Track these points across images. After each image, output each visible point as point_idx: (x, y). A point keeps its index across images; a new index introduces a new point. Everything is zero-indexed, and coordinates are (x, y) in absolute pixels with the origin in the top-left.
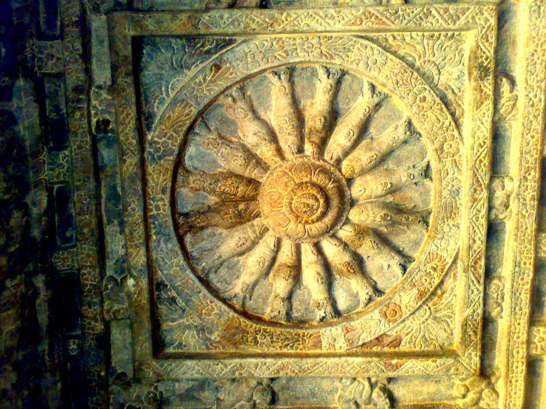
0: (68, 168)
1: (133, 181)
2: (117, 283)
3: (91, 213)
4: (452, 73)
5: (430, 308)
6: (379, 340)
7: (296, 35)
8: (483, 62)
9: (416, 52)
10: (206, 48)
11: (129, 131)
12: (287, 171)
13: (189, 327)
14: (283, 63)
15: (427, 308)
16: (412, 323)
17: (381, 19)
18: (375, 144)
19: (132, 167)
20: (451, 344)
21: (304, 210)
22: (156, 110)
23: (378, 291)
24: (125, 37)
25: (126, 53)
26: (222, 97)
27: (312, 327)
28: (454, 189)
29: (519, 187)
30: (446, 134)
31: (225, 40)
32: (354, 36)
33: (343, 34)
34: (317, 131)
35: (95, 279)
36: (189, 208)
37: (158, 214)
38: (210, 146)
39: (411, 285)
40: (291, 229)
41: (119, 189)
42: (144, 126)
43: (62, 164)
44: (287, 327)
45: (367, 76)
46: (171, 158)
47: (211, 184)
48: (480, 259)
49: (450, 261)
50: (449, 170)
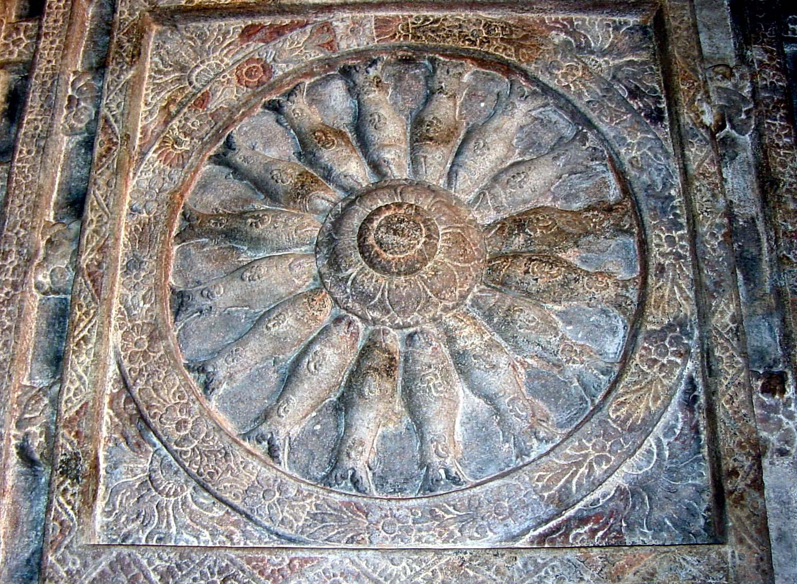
2: (730, 121)
3: (784, 233)
5: (190, 83)
6: (279, 31)
8: (73, 485)
9: (192, 512)
10: (586, 528)
12: (434, 299)
13: (603, 53)
14: (441, 498)
15: (195, 83)
16: (222, 61)
17: (254, 567)
18: (269, 347)
20: (160, 33)
21: (402, 225)
22: (680, 415)
23: (275, 108)
24: (741, 541)
25: (738, 512)
27: (392, 50)
28: (135, 272)
29: (26, 273)
30: (143, 364)
34: (376, 370)
35: (769, 127)
39: (218, 115)
41: (740, 277)
42: (700, 388)
44: (434, 50)
46: (650, 327)
48: (102, 156)
49: (151, 155)
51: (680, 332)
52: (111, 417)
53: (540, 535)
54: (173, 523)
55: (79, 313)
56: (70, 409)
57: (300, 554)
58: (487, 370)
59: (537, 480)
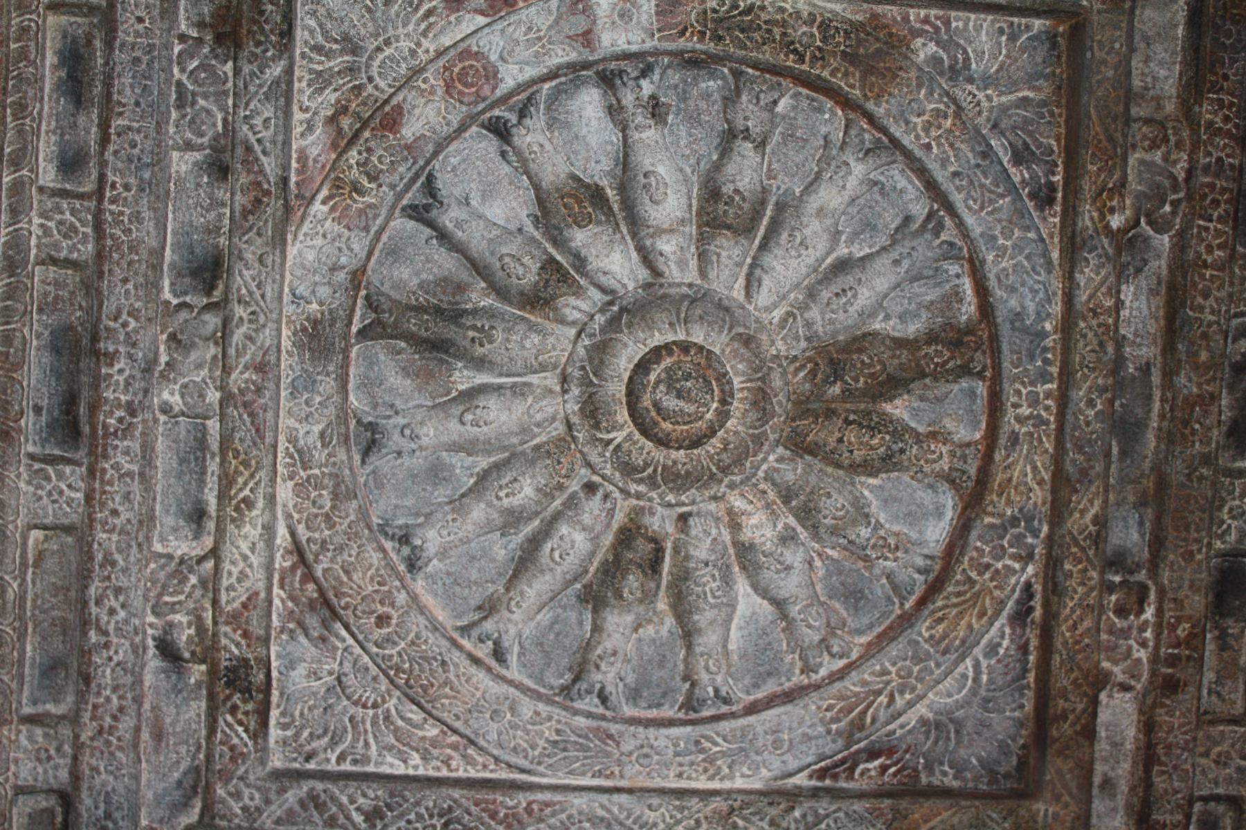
0: (1220, 508)
1: (1084, 472)
2: (1148, 216)
4: (308, 676)
5: (370, 79)
7: (673, 785)
9: (397, 729)
10: (877, 763)
11: (1075, 592)
12: (720, 475)
13: (987, 81)
16: (419, 44)
17: (483, 810)
19: (1081, 506)
22: (1007, 630)
25: (1059, 761)
26: (854, 655)
31: (835, 777)
32: (543, 775)
33: (566, 781)
35: (1199, 233)
36: (956, 387)
37: (1032, 384)
38: (892, 541)
40: (721, 332)
41: (1115, 450)
42: (1038, 597)
43: (1233, 518)
44: (742, 61)
45: (511, 683)
46: (988, 520)
47: (902, 451)
50: (319, 445)
51: (1026, 528)
52: (283, 601)
53: (821, 769)
54: (372, 741)
55: (234, 462)
56: (234, 600)
57: (540, 796)
58: (778, 572)
59: (827, 710)
